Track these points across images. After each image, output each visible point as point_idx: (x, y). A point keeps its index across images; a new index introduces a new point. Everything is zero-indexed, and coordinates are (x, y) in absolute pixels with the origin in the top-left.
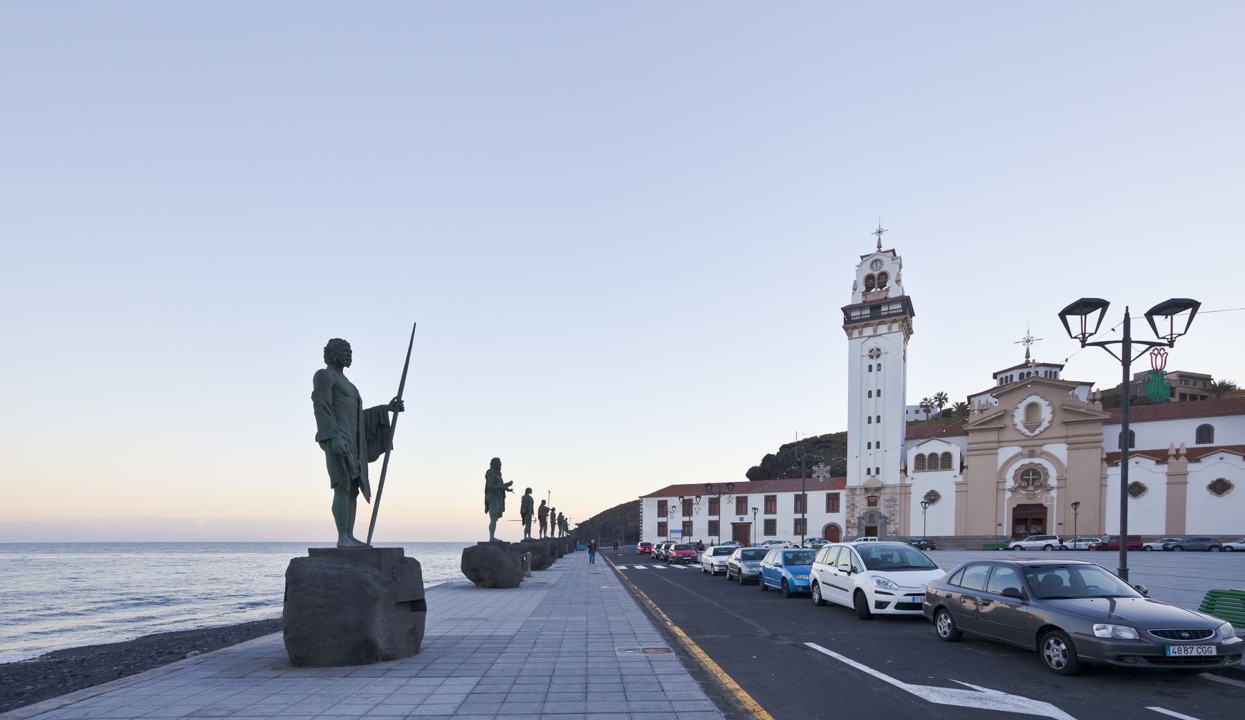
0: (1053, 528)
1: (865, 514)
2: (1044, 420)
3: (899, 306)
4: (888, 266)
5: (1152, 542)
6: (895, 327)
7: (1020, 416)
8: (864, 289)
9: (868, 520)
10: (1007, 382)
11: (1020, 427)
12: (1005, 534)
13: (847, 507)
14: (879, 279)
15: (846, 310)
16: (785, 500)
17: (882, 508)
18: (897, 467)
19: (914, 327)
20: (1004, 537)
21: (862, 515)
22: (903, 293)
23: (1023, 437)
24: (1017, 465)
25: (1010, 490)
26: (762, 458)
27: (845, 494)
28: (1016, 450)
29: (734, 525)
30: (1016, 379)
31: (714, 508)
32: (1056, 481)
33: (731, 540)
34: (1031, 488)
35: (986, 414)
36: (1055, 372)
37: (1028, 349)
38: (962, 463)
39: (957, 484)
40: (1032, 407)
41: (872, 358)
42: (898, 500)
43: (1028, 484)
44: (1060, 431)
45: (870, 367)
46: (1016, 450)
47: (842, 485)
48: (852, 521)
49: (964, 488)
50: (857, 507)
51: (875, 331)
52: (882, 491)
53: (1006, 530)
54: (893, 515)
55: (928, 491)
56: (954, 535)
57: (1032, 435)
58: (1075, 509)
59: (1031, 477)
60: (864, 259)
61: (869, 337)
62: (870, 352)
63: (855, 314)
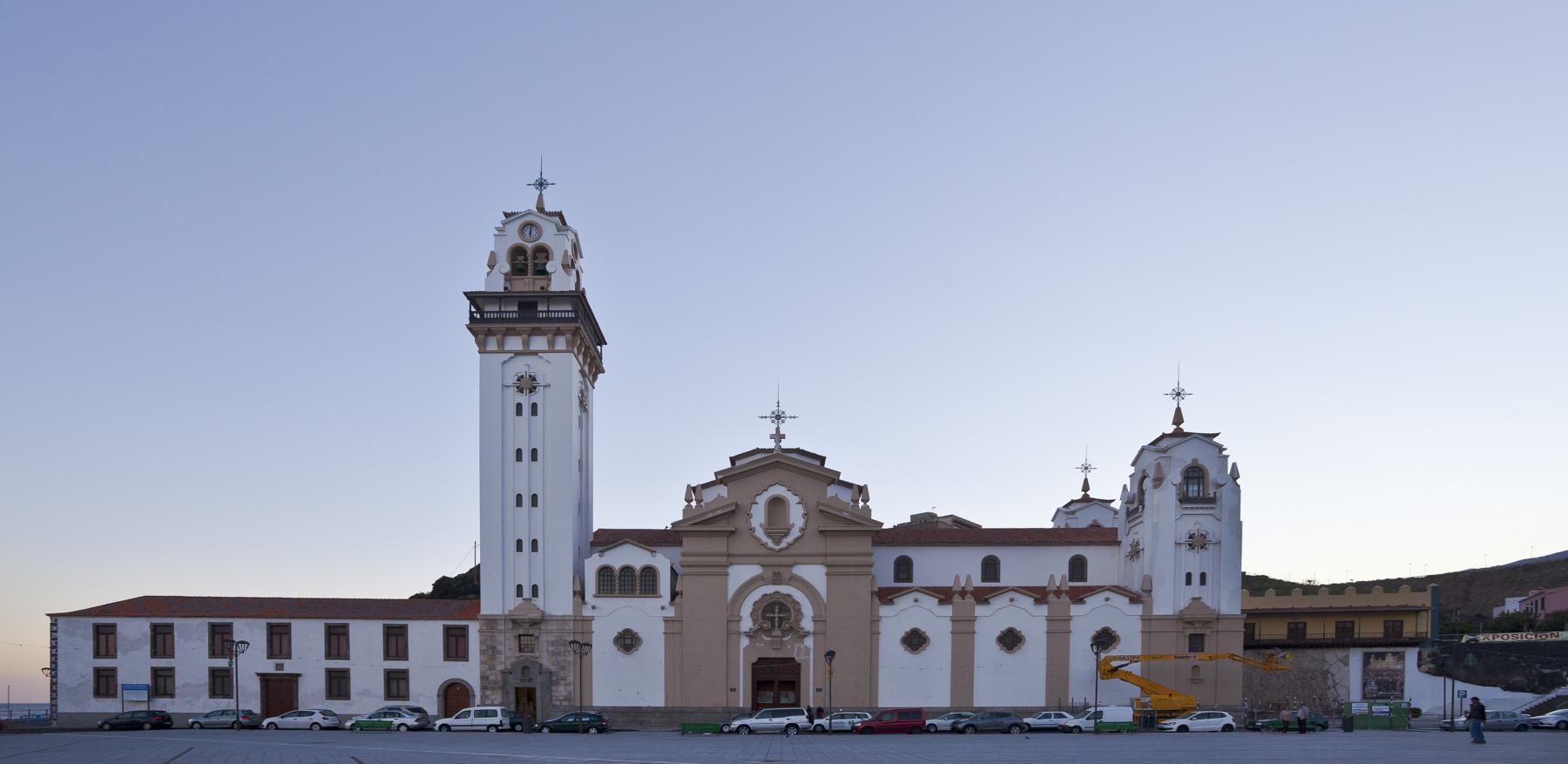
0: (810, 698)
1: (514, 665)
4: (549, 237)
5: (937, 718)
6: (561, 343)
7: (758, 515)
8: (507, 268)
11: (760, 533)
12: (741, 705)
13: (482, 652)
14: (535, 258)
15: (472, 297)
17: (544, 656)
21: (509, 667)
22: (578, 284)
23: (763, 551)
24: (756, 595)
25: (747, 634)
28: (752, 571)
29: (265, 679)
32: (812, 623)
34: (777, 632)
39: (667, 620)
40: (776, 503)
43: (773, 626)
44: (817, 545)
45: (519, 406)
46: (752, 571)
47: (473, 612)
48: (492, 678)
50: (499, 652)
51: (526, 343)
52: (543, 627)
53: (743, 699)
54: (563, 668)
57: (777, 548)
58: (830, 664)
59: (777, 615)
61: (517, 353)
62: (518, 380)
63: (491, 308)
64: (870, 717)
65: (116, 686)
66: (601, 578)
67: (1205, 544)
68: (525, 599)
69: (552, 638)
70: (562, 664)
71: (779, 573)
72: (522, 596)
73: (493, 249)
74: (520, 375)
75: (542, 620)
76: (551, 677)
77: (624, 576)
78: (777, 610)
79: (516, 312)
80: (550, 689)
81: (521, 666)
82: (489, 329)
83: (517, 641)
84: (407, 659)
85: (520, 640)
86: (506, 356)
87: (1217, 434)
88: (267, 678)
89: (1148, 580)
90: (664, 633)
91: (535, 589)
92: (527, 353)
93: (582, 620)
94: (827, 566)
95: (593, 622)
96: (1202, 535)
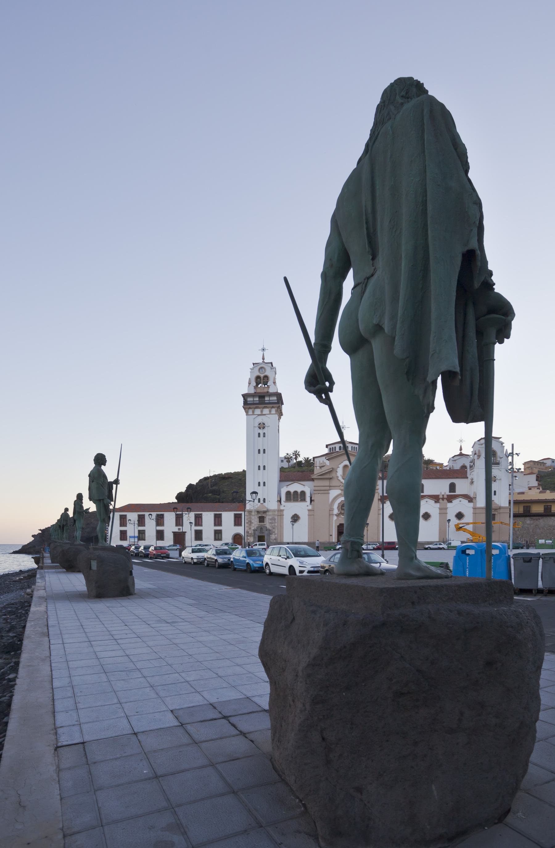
1: (257, 528)
3: (275, 398)
4: (268, 373)
6: (273, 411)
8: (255, 384)
9: (259, 531)
11: (340, 478)
12: (334, 541)
14: (264, 379)
15: (245, 396)
16: (208, 517)
18: (276, 499)
19: (283, 411)
20: (333, 543)
21: (256, 528)
25: (336, 515)
26: (186, 486)
29: (175, 534)
31: (160, 520)
33: (172, 544)
35: (323, 469)
38: (311, 498)
39: (309, 510)
41: (260, 429)
42: (277, 519)
45: (259, 434)
48: (250, 532)
49: (312, 513)
50: (252, 523)
51: (262, 412)
54: (274, 528)
55: (293, 514)
56: (307, 541)
60: (255, 365)
61: (258, 415)
62: (259, 425)
63: (250, 399)
64: (378, 545)
65: (127, 536)
67: (496, 480)
68: (261, 504)
69: (270, 517)
70: (274, 527)
72: (260, 502)
73: (250, 377)
74: (259, 423)
75: (267, 511)
76: (270, 532)
79: (257, 401)
80: (269, 536)
81: (260, 528)
83: (259, 519)
84: (222, 526)
86: (255, 416)
87: (501, 438)
88: (175, 533)
89: (475, 494)
90: (308, 515)
91: (264, 499)
92: (262, 415)
95: (284, 511)
96: (494, 476)
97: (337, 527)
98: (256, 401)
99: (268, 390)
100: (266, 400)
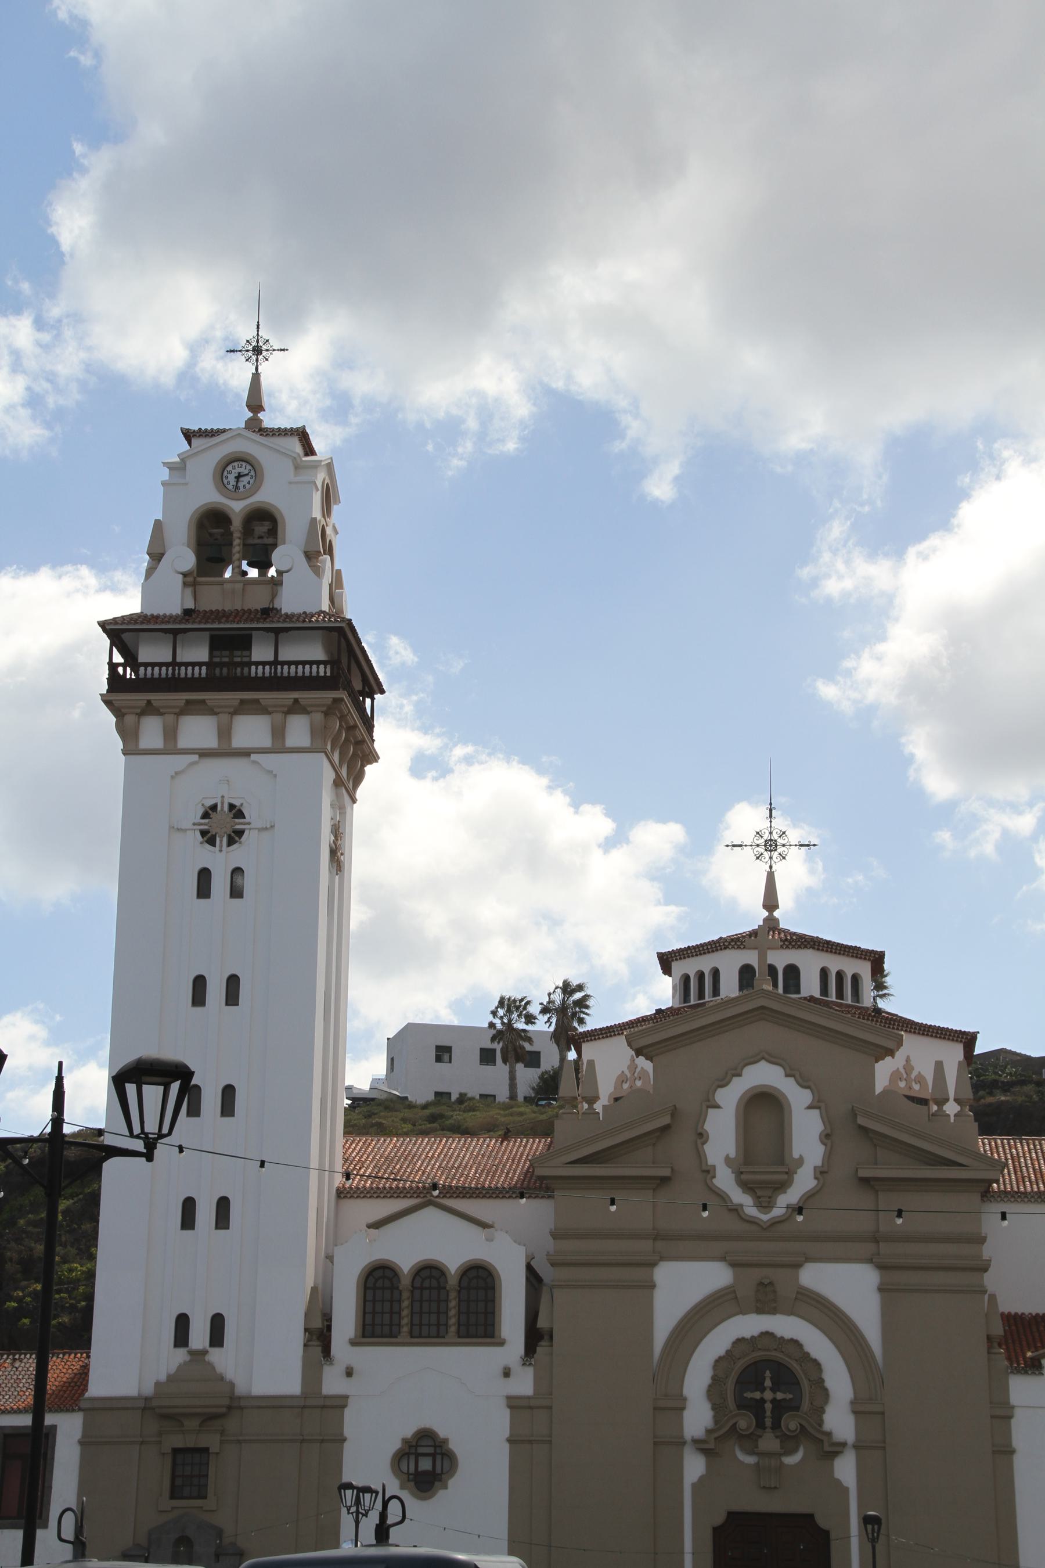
2: (800, 1161)
3: (316, 652)
8: (188, 560)
10: (701, 994)
11: (725, 1180)
25: (701, 1446)
27: (78, 1434)
30: (730, 987)
36: (856, 979)
37: (771, 878)
39: (514, 1404)
41: (212, 842)
45: (204, 877)
51: (225, 733)
55: (409, 1432)
57: (765, 1217)
59: (768, 1395)
60: (194, 441)
61: (205, 754)
62: (206, 815)
66: (370, 1293)
68: (193, 1353)
71: (771, 1284)
73: (160, 517)
74: (209, 803)
75: (230, 1408)
77: (422, 1288)
78: (768, 1383)
82: (149, 702)
85: (174, 1464)
90: (509, 1440)
91: (218, 1323)
92: (225, 751)
93: (323, 1407)
94: (881, 1267)
95: (347, 1411)
97: (708, 1535)
98: (193, 664)
99: (272, 601)
100: (255, 657)
